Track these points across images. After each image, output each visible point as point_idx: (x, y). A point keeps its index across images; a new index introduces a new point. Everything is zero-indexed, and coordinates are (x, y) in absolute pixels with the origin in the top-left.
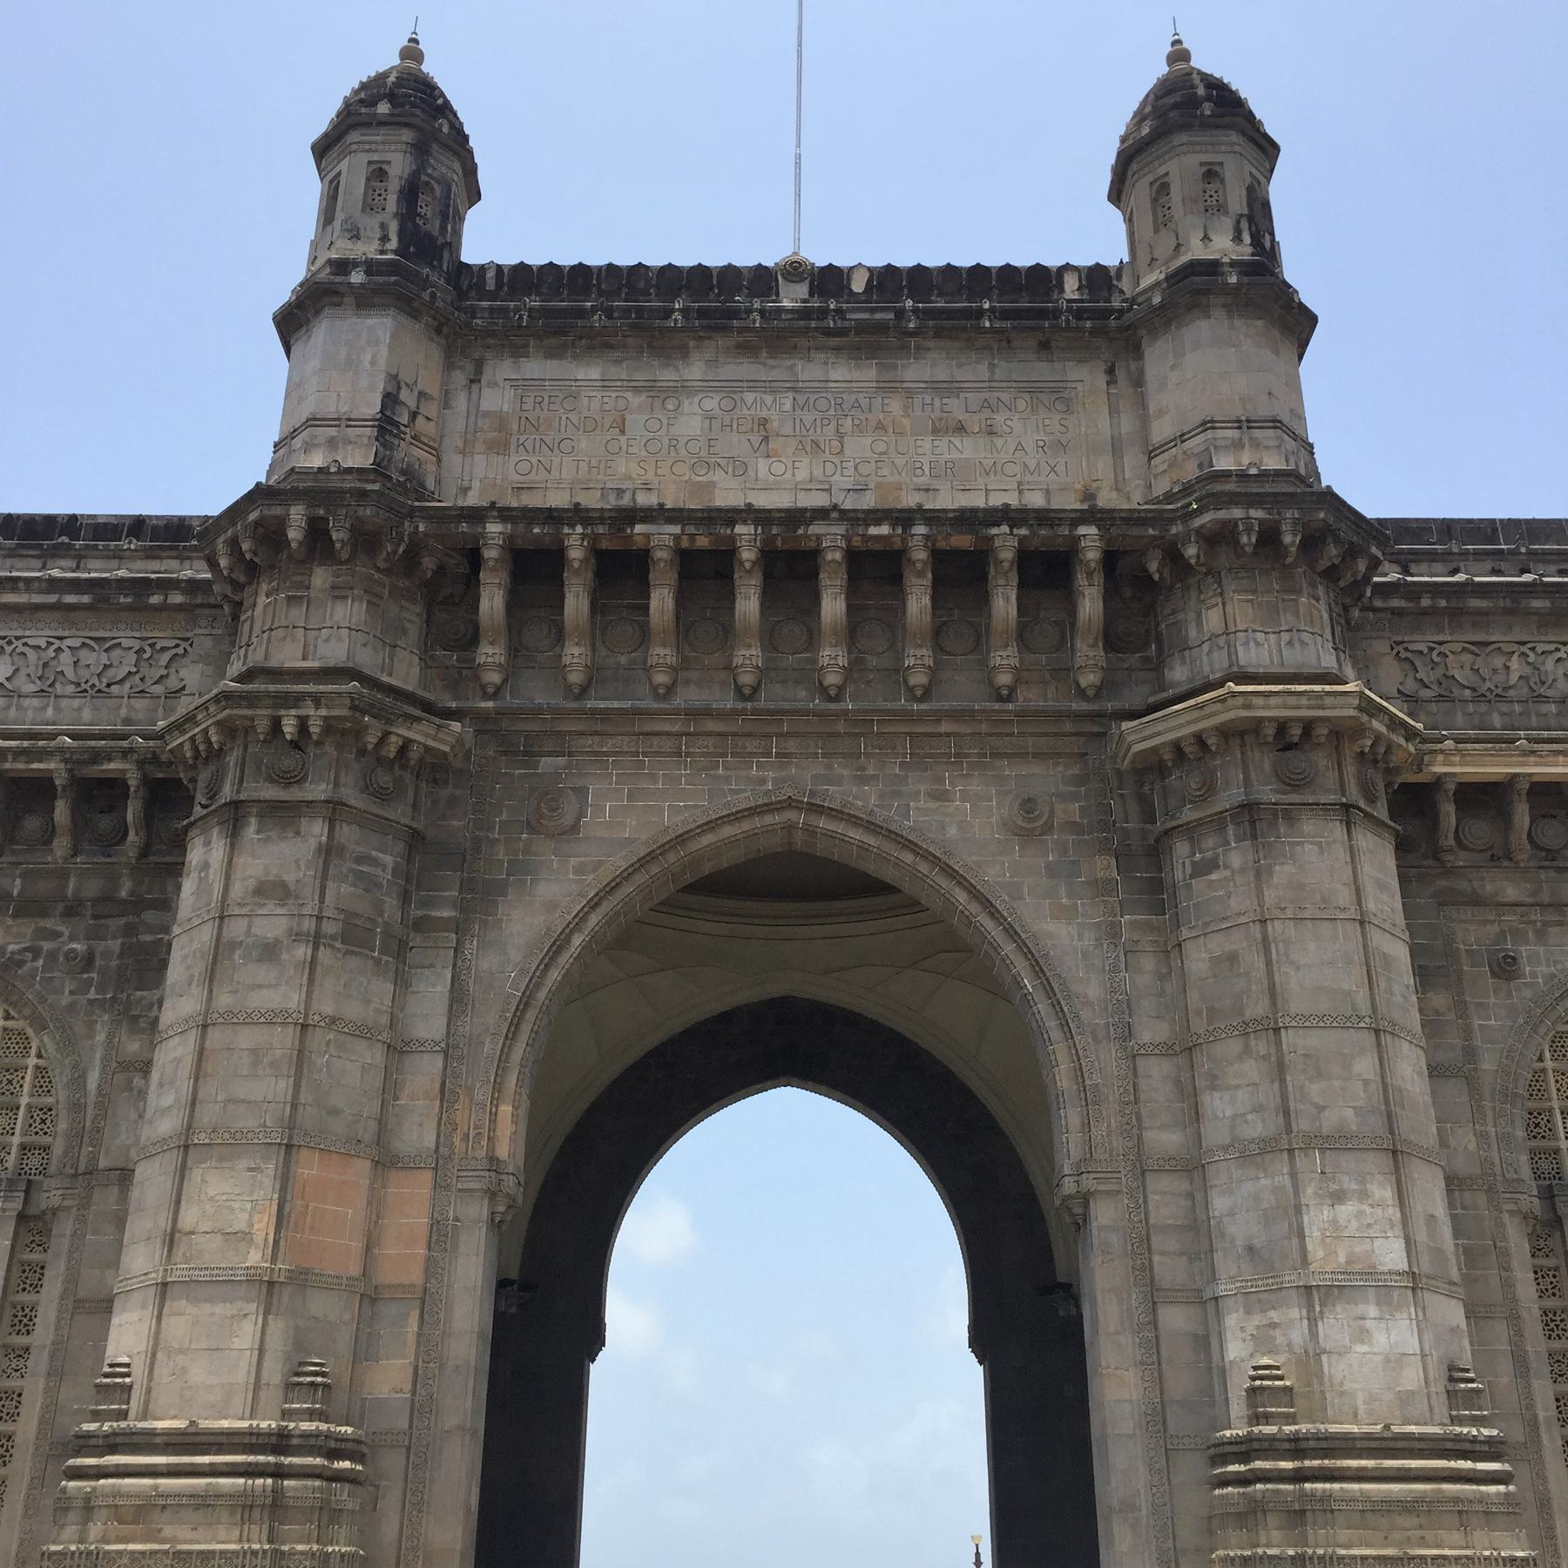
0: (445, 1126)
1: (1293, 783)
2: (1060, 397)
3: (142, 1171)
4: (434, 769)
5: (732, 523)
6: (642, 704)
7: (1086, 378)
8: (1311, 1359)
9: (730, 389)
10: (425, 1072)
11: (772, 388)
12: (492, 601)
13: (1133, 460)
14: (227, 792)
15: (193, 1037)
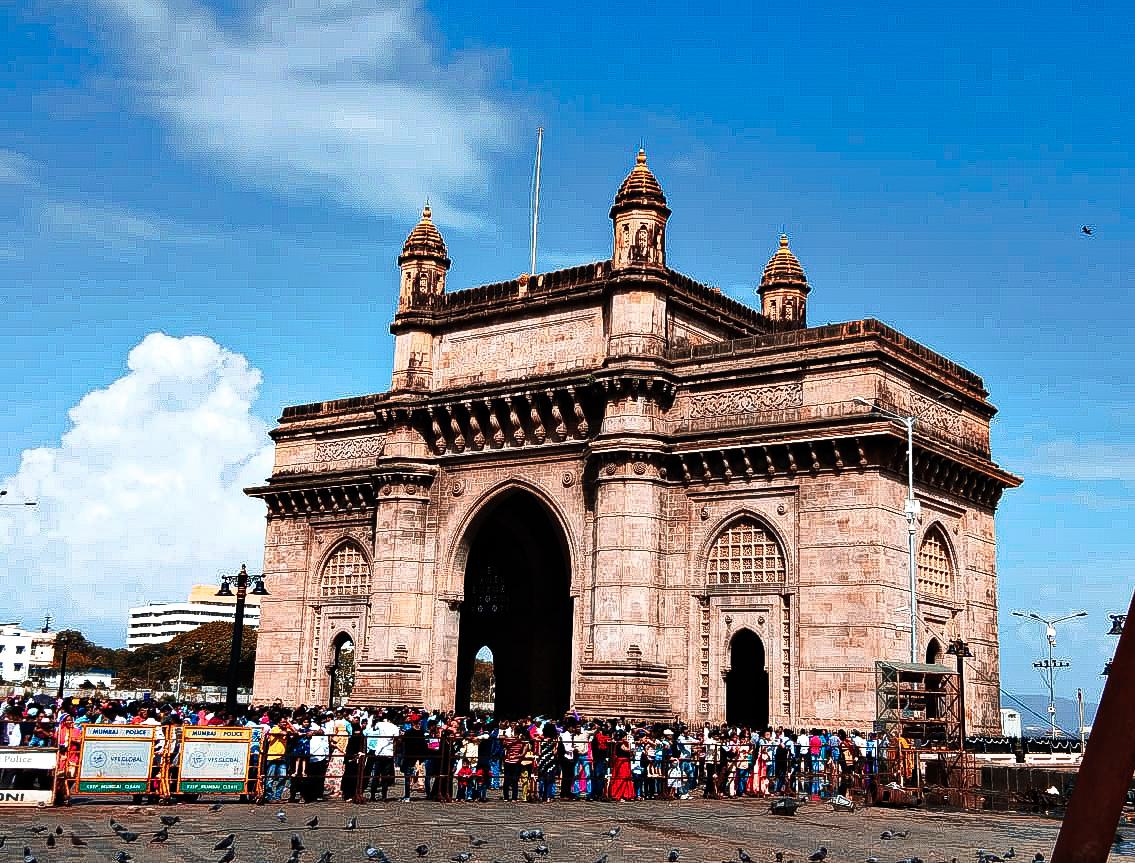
4: (426, 481)
10: (428, 569)
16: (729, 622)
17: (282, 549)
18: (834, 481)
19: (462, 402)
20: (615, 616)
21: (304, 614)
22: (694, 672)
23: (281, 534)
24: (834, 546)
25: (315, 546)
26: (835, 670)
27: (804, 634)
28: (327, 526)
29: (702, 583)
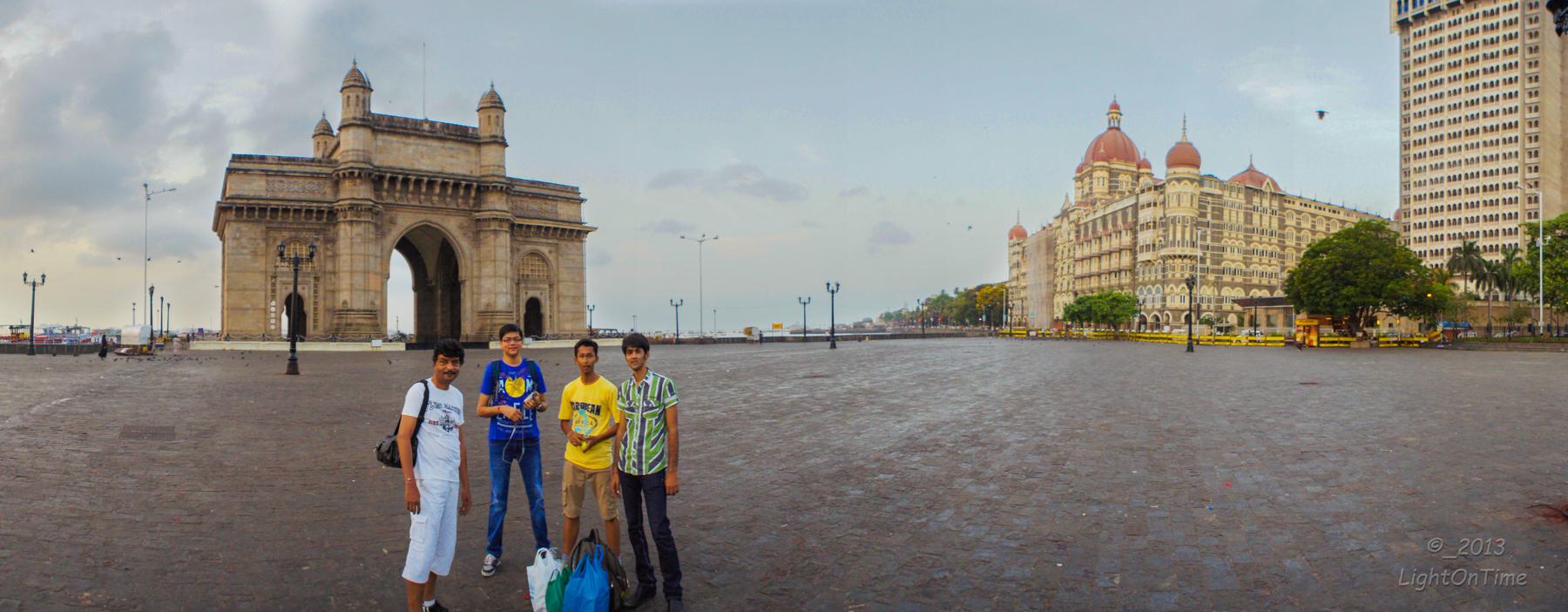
0: (382, 268)
1: (501, 226)
2: (468, 152)
3: (342, 275)
4: (377, 214)
5: (424, 176)
6: (406, 203)
7: (472, 149)
8: (495, 302)
9: (417, 145)
10: (379, 260)
11: (424, 146)
12: (386, 185)
13: (478, 166)
14: (348, 219)
15: (349, 257)
16: (526, 293)
17: (244, 241)
18: (570, 244)
19: (410, 177)
20: (504, 290)
21: (266, 280)
22: (515, 314)
23: (241, 232)
24: (572, 268)
25: (271, 241)
26: (572, 312)
27: (561, 299)
28: (279, 229)
29: (516, 278)
